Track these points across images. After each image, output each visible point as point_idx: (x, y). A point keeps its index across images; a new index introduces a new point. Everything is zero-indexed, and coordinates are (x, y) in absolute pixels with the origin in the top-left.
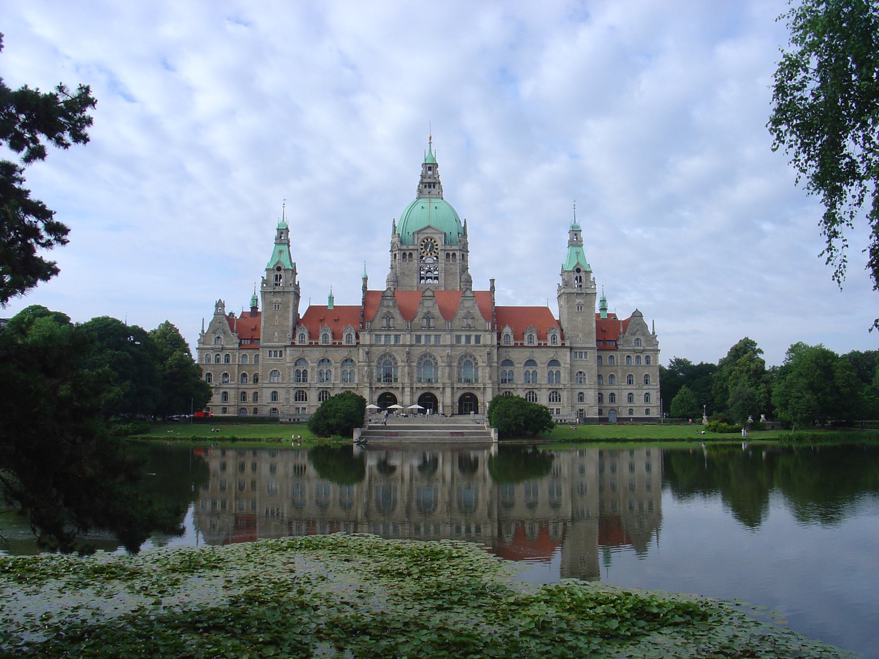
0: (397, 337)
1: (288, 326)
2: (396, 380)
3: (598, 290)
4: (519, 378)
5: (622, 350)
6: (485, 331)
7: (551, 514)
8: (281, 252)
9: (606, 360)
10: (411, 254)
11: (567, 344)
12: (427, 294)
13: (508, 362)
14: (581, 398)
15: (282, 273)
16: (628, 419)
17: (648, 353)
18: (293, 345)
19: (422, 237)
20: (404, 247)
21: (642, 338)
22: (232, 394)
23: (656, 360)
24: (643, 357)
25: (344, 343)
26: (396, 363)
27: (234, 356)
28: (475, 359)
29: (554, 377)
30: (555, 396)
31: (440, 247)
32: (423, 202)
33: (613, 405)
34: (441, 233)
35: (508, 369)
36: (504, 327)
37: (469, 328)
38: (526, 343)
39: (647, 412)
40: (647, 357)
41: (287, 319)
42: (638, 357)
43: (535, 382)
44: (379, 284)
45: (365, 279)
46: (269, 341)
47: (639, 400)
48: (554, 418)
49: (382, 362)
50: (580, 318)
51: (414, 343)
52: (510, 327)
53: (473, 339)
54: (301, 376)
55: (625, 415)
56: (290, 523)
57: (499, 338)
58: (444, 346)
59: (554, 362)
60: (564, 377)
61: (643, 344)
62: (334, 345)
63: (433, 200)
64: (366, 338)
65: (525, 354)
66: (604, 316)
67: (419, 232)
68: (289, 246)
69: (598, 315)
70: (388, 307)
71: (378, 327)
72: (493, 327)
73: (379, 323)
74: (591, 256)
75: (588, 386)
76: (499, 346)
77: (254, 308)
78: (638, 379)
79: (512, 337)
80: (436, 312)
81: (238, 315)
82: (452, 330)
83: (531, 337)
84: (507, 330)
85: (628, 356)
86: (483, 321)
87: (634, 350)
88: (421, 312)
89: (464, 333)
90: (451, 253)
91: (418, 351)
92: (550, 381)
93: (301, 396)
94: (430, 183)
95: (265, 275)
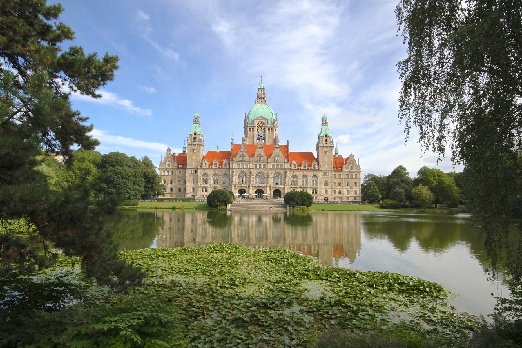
3: (335, 145)
4: (300, 183)
8: (196, 127)
10: (253, 129)
11: (321, 169)
13: (295, 176)
16: (347, 202)
19: (258, 121)
23: (359, 176)
24: (354, 174)
25: (223, 167)
27: (175, 172)
30: (315, 191)
34: (266, 119)
41: (199, 156)
42: (352, 175)
44: (238, 142)
47: (352, 193)
48: (314, 200)
54: (206, 181)
55: (345, 199)
57: (291, 165)
59: (315, 176)
66: (337, 156)
67: (256, 119)
69: (334, 156)
72: (288, 161)
77: (184, 151)
78: (352, 184)
80: (263, 154)
81: (177, 154)
83: (305, 165)
84: (294, 162)
87: (350, 172)
88: (257, 154)
92: (313, 185)
93: (205, 189)
95: (189, 136)
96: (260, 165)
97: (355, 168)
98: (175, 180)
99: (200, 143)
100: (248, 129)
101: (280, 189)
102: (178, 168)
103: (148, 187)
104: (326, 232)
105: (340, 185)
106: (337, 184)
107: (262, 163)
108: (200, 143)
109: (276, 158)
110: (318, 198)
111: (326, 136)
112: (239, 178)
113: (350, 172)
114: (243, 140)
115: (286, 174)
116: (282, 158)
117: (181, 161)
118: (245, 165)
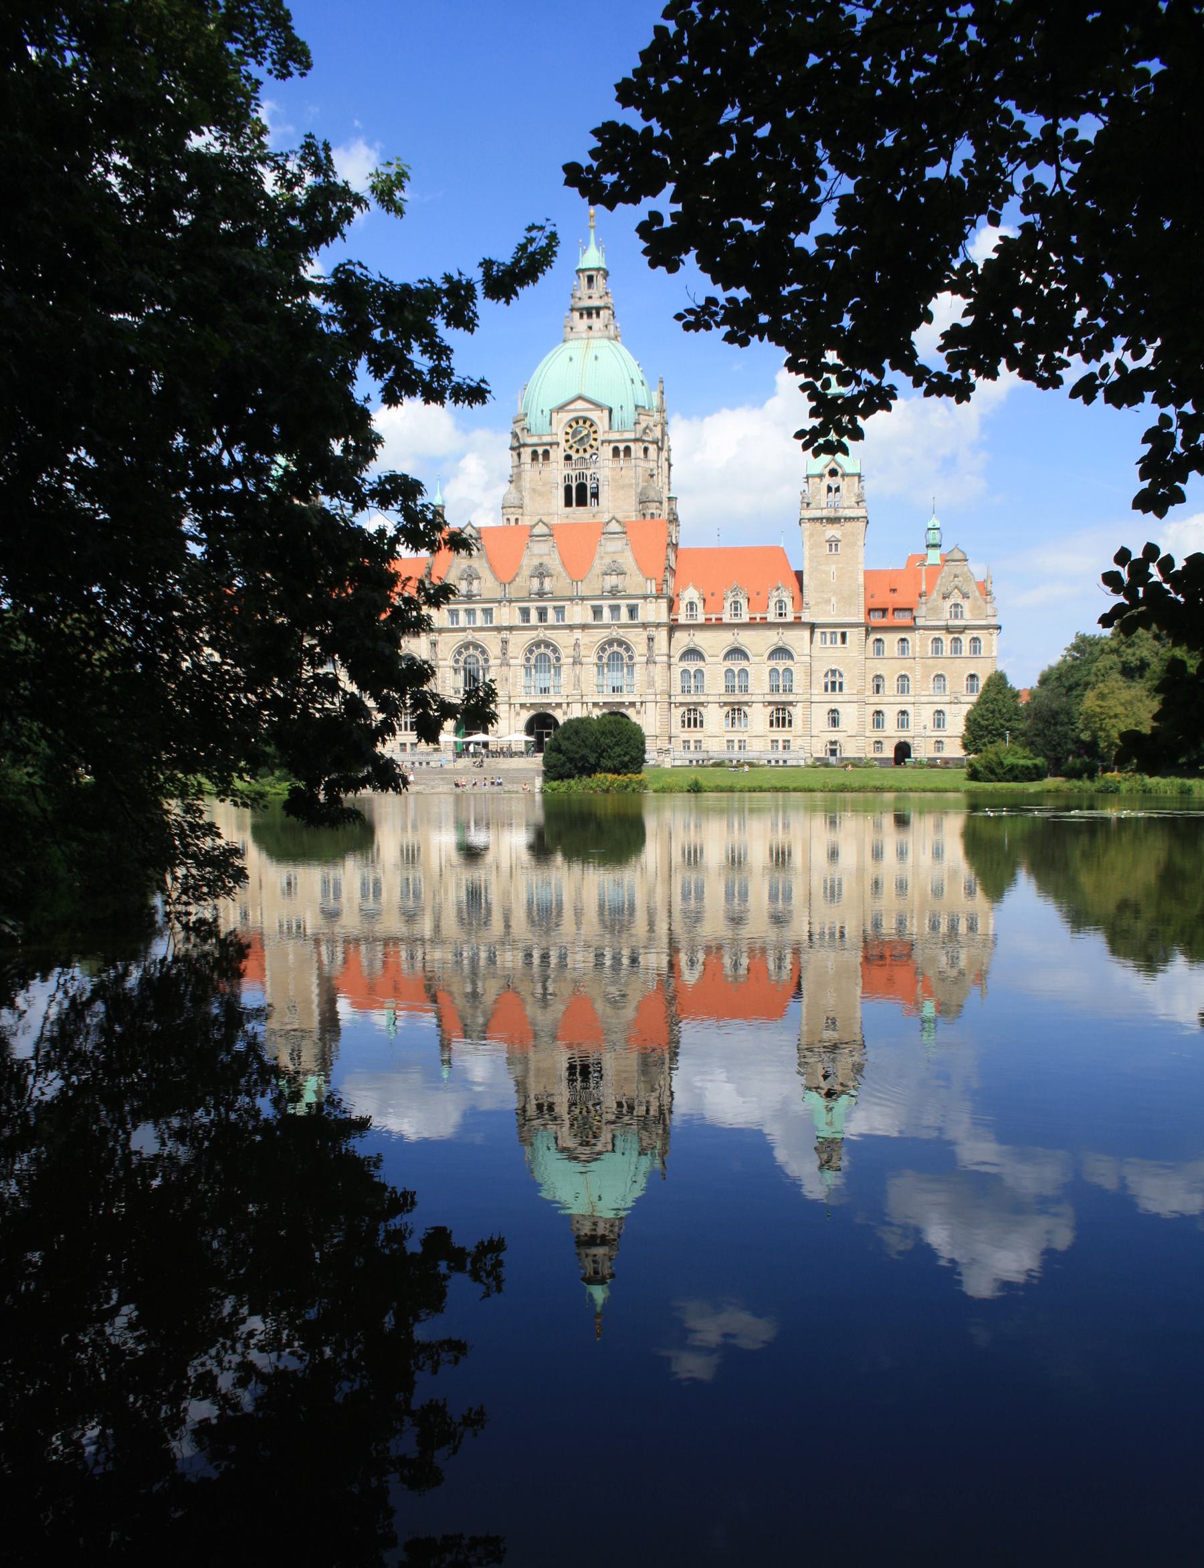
0: (488, 612)
6: (645, 597)
10: (546, 453)
12: (536, 531)
13: (693, 653)
17: (975, 633)
19: (566, 417)
20: (535, 440)
21: (966, 604)
26: (486, 660)
28: (628, 649)
29: (781, 682)
31: (601, 436)
33: (901, 734)
34: (598, 406)
35: (692, 666)
36: (685, 588)
40: (975, 640)
42: (956, 640)
43: (745, 689)
49: (462, 659)
50: (833, 568)
52: (696, 588)
53: (624, 612)
56: (317, 942)
59: (780, 652)
61: (967, 614)
65: (725, 640)
67: (561, 408)
75: (846, 698)
79: (700, 605)
80: (554, 563)
82: (583, 599)
84: (691, 594)
85: (937, 640)
86: (641, 579)
87: (948, 629)
88: (528, 563)
89: (605, 604)
90: (622, 446)
91: (519, 641)
96: (542, 614)
97: (975, 608)
104: (833, 892)
105: (903, 689)
106: (890, 685)
107: (550, 605)
109: (612, 580)
110: (794, 745)
112: (456, 670)
113: (948, 629)
116: (636, 582)
118: (479, 614)
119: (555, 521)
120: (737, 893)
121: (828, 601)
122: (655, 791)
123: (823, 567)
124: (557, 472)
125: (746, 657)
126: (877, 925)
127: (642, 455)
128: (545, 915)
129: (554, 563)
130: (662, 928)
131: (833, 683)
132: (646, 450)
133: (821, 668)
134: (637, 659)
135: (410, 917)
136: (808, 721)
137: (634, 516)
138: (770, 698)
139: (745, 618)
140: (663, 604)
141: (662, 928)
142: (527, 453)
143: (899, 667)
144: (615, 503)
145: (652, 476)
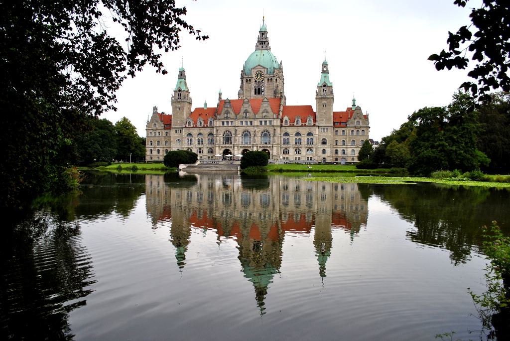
1: (183, 118)
2: (231, 143)
5: (350, 127)
7: (307, 209)
8: (181, 82)
9: (340, 132)
11: (317, 124)
12: (245, 101)
13: (286, 134)
14: (324, 151)
15: (181, 92)
18: (186, 127)
19: (255, 71)
20: (247, 76)
21: (361, 121)
22: (161, 150)
24: (360, 131)
26: (231, 135)
32: (258, 52)
34: (264, 68)
37: (265, 117)
38: (295, 124)
39: (353, 159)
42: (358, 131)
45: (220, 94)
46: (176, 126)
51: (239, 125)
55: (350, 161)
58: (254, 126)
59: (310, 134)
60: (315, 141)
61: (361, 124)
62: (204, 127)
63: (263, 51)
64: (218, 123)
67: (254, 68)
68: (185, 79)
70: (228, 108)
71: (223, 117)
73: (223, 116)
74: (333, 78)
75: (328, 146)
76: (281, 126)
79: (289, 121)
80: (250, 109)
83: (298, 122)
84: (286, 118)
87: (355, 128)
88: (243, 109)
89: (263, 120)
90: (270, 79)
91: (240, 131)
92: (308, 143)
94: (263, 42)
98: (162, 140)
99: (185, 100)
100: (245, 81)
101: (268, 149)
102: (165, 128)
103: (125, 148)
104: (323, 198)
105: (344, 144)
106: (340, 143)
108: (185, 100)
109: (264, 114)
111: (325, 86)
112: (224, 138)
113: (355, 128)
114: (239, 94)
115: (274, 132)
116: (271, 114)
117: (162, 121)
119: (252, 98)
120: (297, 198)
121: (323, 120)
122: (271, 171)
123: (322, 111)
124: (253, 85)
125: (300, 135)
126: (336, 207)
127: (275, 81)
128: (246, 204)
129: (250, 109)
130: (277, 208)
131: (324, 142)
132: (276, 79)
133: (321, 138)
134: (271, 135)
135: (211, 202)
136: (317, 152)
137: (273, 97)
138: (306, 146)
139: (300, 125)
140: (279, 121)
141: (277, 208)
142: (245, 80)
143: (342, 138)
144: (267, 93)
145: (278, 86)
